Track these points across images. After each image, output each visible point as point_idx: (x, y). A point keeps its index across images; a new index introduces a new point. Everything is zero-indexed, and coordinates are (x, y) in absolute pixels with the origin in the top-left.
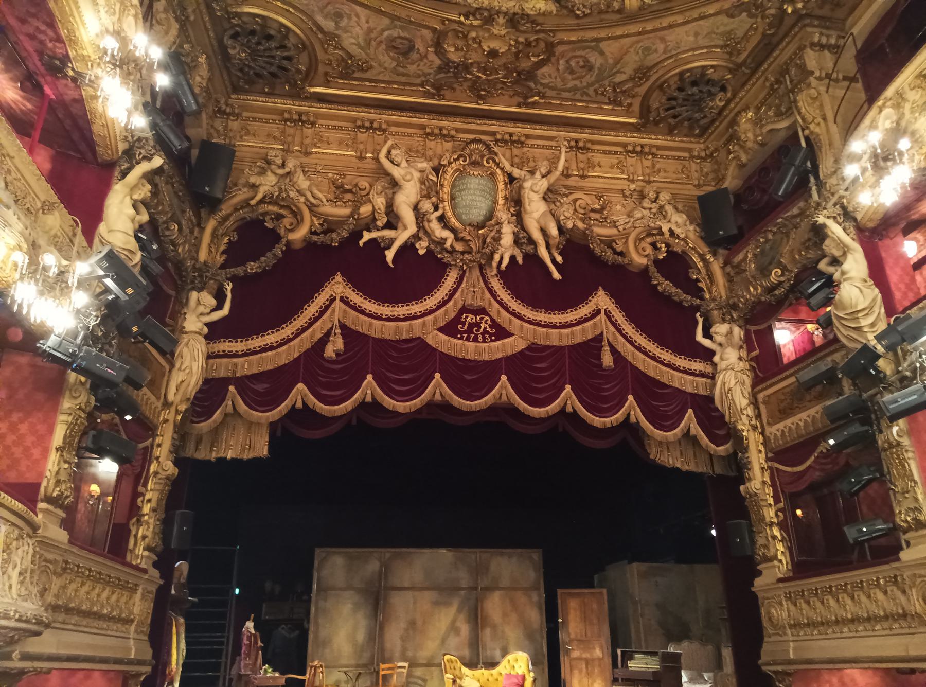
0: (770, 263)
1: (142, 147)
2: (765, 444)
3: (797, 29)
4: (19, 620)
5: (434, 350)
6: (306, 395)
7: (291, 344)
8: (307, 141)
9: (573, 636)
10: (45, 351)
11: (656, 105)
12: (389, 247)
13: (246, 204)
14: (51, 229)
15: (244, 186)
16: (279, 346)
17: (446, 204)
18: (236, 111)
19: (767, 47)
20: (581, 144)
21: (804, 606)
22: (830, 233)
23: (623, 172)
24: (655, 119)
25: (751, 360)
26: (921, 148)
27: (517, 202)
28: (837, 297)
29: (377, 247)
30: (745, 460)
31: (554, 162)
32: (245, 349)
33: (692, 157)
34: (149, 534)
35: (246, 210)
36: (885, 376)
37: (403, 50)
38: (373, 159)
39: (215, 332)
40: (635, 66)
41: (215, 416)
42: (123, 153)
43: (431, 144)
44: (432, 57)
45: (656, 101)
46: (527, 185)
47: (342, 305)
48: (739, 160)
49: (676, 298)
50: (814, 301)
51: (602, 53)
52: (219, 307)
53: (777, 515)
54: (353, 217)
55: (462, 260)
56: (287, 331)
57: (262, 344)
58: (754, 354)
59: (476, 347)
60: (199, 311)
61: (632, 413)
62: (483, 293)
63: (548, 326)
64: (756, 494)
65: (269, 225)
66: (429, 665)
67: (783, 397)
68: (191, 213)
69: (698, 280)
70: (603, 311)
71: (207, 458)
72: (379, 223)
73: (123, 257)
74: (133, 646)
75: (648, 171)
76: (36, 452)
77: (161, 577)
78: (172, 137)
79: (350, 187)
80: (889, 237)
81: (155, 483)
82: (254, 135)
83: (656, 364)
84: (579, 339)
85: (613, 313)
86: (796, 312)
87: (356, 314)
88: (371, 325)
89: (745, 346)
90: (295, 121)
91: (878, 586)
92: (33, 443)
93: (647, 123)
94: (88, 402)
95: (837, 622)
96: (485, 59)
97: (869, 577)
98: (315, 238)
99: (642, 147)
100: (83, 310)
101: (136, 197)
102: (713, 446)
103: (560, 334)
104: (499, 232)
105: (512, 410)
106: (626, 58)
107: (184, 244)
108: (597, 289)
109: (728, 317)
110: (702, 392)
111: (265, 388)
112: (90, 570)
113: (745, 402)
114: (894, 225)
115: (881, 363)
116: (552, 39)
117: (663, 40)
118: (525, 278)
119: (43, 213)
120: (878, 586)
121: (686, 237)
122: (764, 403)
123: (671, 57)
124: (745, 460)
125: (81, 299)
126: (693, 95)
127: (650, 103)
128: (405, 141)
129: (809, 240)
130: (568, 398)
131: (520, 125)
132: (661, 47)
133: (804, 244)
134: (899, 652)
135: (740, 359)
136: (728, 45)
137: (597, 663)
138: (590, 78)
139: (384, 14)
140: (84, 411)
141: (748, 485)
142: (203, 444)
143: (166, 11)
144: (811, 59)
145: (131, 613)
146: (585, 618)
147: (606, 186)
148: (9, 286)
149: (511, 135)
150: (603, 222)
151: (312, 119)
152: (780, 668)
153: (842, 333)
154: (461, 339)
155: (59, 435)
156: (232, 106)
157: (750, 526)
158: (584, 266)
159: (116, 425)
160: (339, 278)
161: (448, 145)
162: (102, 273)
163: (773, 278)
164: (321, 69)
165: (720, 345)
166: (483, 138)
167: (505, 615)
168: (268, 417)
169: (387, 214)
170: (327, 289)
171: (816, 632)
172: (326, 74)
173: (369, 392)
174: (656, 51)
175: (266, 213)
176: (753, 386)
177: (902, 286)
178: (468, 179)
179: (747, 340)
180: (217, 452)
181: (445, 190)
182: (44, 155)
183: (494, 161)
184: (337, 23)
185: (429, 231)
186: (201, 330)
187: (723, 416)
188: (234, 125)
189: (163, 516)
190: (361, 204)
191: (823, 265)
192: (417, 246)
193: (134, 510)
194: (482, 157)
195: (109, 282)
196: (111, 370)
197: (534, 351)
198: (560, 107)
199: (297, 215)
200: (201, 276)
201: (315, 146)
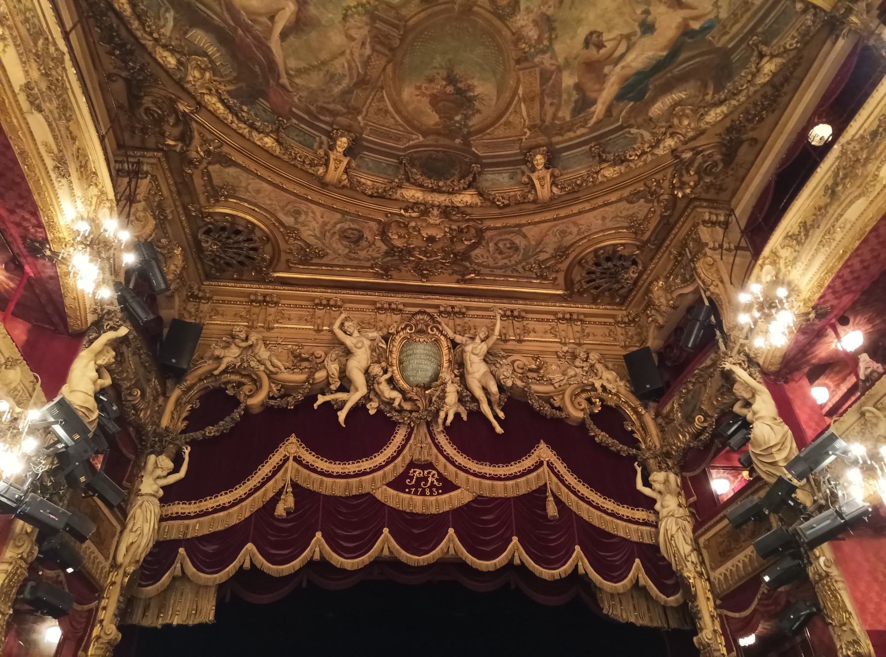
0: (693, 411)
1: (111, 320)
2: (712, 590)
3: (689, 210)
5: (383, 505)
6: (254, 555)
7: (243, 504)
8: (270, 318)
11: (578, 278)
12: (341, 409)
13: (210, 374)
14: (10, 383)
15: (210, 359)
17: (395, 368)
19: (666, 226)
20: (516, 313)
23: (556, 336)
24: (579, 290)
27: (460, 365)
28: (751, 436)
29: (331, 409)
30: (695, 609)
31: (491, 329)
32: (198, 510)
33: (617, 323)
35: (210, 380)
36: (805, 507)
37: (355, 239)
38: (329, 331)
39: (170, 495)
40: (555, 246)
42: (92, 324)
43: (382, 317)
44: (379, 243)
45: (578, 275)
46: (469, 348)
47: (296, 465)
48: (657, 322)
49: (613, 448)
51: (525, 236)
52: (176, 470)
54: (308, 381)
55: (409, 418)
56: (240, 491)
57: (215, 505)
58: (692, 500)
59: (424, 501)
60: (157, 473)
61: (580, 564)
62: (430, 448)
63: (492, 478)
64: (709, 645)
65: (230, 392)
67: (720, 540)
68: (157, 382)
69: (633, 432)
70: (545, 463)
71: (154, 625)
72: (333, 387)
73: (81, 413)
75: (578, 335)
78: (139, 311)
79: (307, 356)
80: (793, 380)
81: (96, 648)
82: (222, 315)
83: (599, 513)
84: (523, 491)
85: (556, 465)
86: (728, 459)
87: (309, 472)
88: (322, 482)
89: (683, 492)
90: (259, 302)
93: (572, 293)
94: (30, 551)
96: (425, 244)
98: (272, 402)
100: (34, 459)
101: (100, 362)
103: (505, 487)
106: (546, 239)
107: (146, 409)
109: (664, 466)
110: (647, 540)
114: (798, 369)
115: (800, 495)
116: (481, 226)
117: (575, 224)
118: (470, 434)
119: (6, 368)
121: (618, 392)
122: (705, 547)
123: (585, 238)
124: (695, 609)
125: (31, 444)
126: (609, 269)
128: (358, 315)
129: (723, 386)
130: (515, 550)
132: (575, 230)
133: (719, 390)
135: (680, 505)
136: (632, 226)
138: (516, 258)
139: (336, 210)
141: (700, 635)
142: (151, 611)
143: (144, 210)
144: (705, 233)
147: (542, 349)
149: (453, 307)
150: (540, 380)
151: (275, 300)
153: (762, 469)
154: (409, 493)
159: (61, 582)
160: (293, 439)
161: (397, 317)
162: (52, 420)
164: (284, 257)
165: (660, 492)
166: (428, 310)
168: (215, 578)
169: (340, 379)
170: (281, 450)
172: (288, 261)
173: (317, 549)
174: (571, 233)
175: (229, 382)
176: (694, 531)
177: (813, 424)
178: (414, 346)
179: (684, 486)
181: (394, 356)
183: (438, 329)
184: (296, 219)
185: (379, 393)
186: (157, 492)
187: (670, 565)
188: (205, 307)
190: (317, 371)
191: (737, 408)
192: (368, 406)
194: (427, 326)
195: (59, 429)
197: (480, 504)
198: (494, 282)
199: (257, 383)
200: (161, 441)
201: (277, 322)
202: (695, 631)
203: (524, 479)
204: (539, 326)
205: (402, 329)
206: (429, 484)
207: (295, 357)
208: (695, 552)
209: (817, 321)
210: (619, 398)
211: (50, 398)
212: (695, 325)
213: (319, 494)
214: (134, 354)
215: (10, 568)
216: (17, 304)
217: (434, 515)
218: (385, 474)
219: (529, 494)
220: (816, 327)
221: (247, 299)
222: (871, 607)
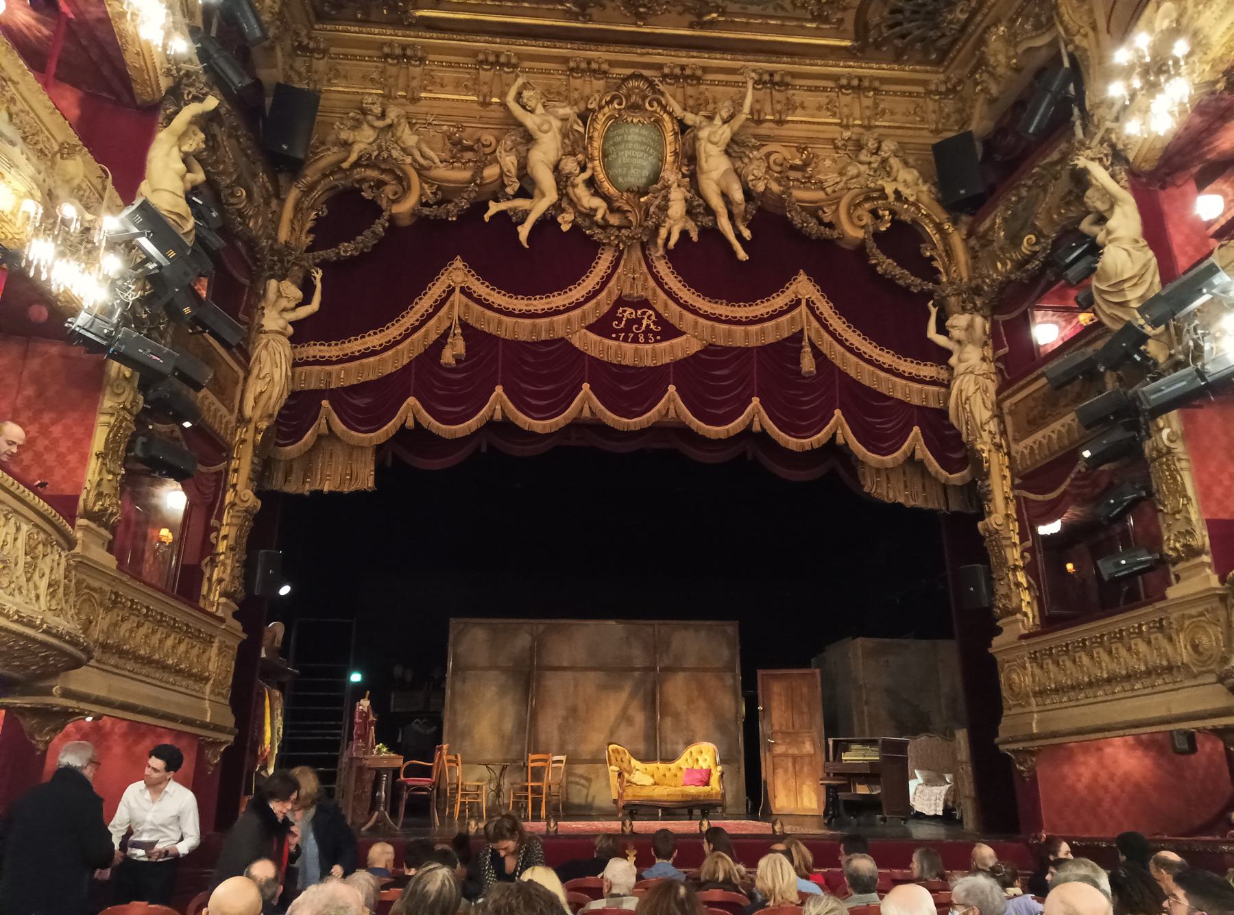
0: (1022, 228)
1: (192, 85)
2: (1010, 467)
4: (47, 632)
5: (581, 354)
6: (418, 411)
7: (399, 347)
8: (414, 83)
9: (776, 727)
10: (74, 331)
11: (876, 20)
12: (522, 222)
13: (336, 168)
15: (334, 145)
16: (382, 350)
17: (597, 163)
18: (322, 46)
20: (777, 78)
21: (1051, 666)
22: (1094, 181)
23: (834, 115)
24: (875, 40)
25: (998, 360)
26: (1205, 53)
27: (690, 160)
28: (1099, 265)
29: (507, 222)
31: (738, 104)
32: (341, 354)
34: (227, 577)
36: (1156, 364)
39: (302, 333)
41: (306, 437)
42: (167, 93)
43: (577, 83)
46: (703, 134)
47: (464, 298)
49: (901, 282)
50: (1071, 273)
52: (306, 301)
53: (1023, 557)
55: (617, 237)
57: (362, 348)
58: (1002, 352)
59: (636, 349)
60: (281, 306)
61: (839, 432)
62: (646, 280)
63: (729, 321)
64: (997, 532)
65: (367, 195)
66: (594, 761)
67: (1032, 404)
68: (266, 179)
69: (932, 258)
70: (804, 302)
71: (300, 491)
72: (509, 190)
74: (211, 707)
75: (868, 113)
76: (73, 459)
77: (244, 631)
82: (346, 77)
83: (872, 368)
84: (771, 339)
85: (818, 304)
86: (1063, 297)
87: (483, 309)
88: (500, 322)
89: (990, 342)
91: (1140, 633)
92: (68, 448)
94: (134, 401)
95: (1090, 684)
97: (1130, 623)
98: (426, 211)
99: (860, 79)
100: (119, 283)
101: (185, 148)
102: (944, 473)
103: (747, 334)
104: (666, 199)
105: (684, 432)
107: (256, 216)
108: (797, 273)
109: (969, 306)
111: (368, 403)
112: (148, 608)
113: (987, 414)
114: (1184, 167)
115: (1152, 348)
118: (702, 261)
119: (62, 158)
120: (1140, 633)
122: (1011, 413)
125: (113, 264)
127: (869, 16)
128: (541, 80)
129: (1070, 192)
131: (695, 54)
133: (1063, 198)
134: (1161, 712)
135: (984, 359)
137: (807, 760)
140: (131, 414)
141: (987, 520)
142: (294, 475)
145: (206, 669)
146: (792, 705)
148: (23, 245)
149: (683, 68)
150: (806, 183)
151: (419, 54)
152: (1020, 746)
154: (617, 339)
155: (99, 440)
156: (315, 39)
157: (989, 571)
158: (780, 242)
159: (177, 439)
160: (458, 263)
161: (599, 84)
162: (137, 231)
163: (1025, 248)
165: (959, 342)
166: (646, 73)
167: (690, 701)
170: (443, 278)
171: (1065, 699)
173: (498, 407)
175: (363, 180)
176: (998, 393)
177: (1190, 250)
180: (311, 484)
181: (595, 144)
182: (71, 98)
183: (660, 103)
187: (959, 435)
188: (321, 65)
189: (244, 557)
190: (485, 166)
191: (1085, 226)
192: (560, 219)
193: (208, 548)
194: (644, 98)
196: (158, 355)
197: (711, 355)
198: (746, 27)
200: (281, 261)
201: (425, 90)
202: (981, 515)
203: (773, 323)
204: (812, 100)
205: (608, 103)
206: (643, 328)
207: (454, 144)
208: (996, 420)
209: (1226, 95)
210: (919, 209)
211: (128, 201)
212: (1045, 96)
213: (497, 338)
214: (229, 136)
215: (112, 420)
216: (59, 62)
217: (650, 368)
218: (584, 313)
219: (779, 343)
220: (1223, 104)
221: (377, 53)
222: (1218, 491)
